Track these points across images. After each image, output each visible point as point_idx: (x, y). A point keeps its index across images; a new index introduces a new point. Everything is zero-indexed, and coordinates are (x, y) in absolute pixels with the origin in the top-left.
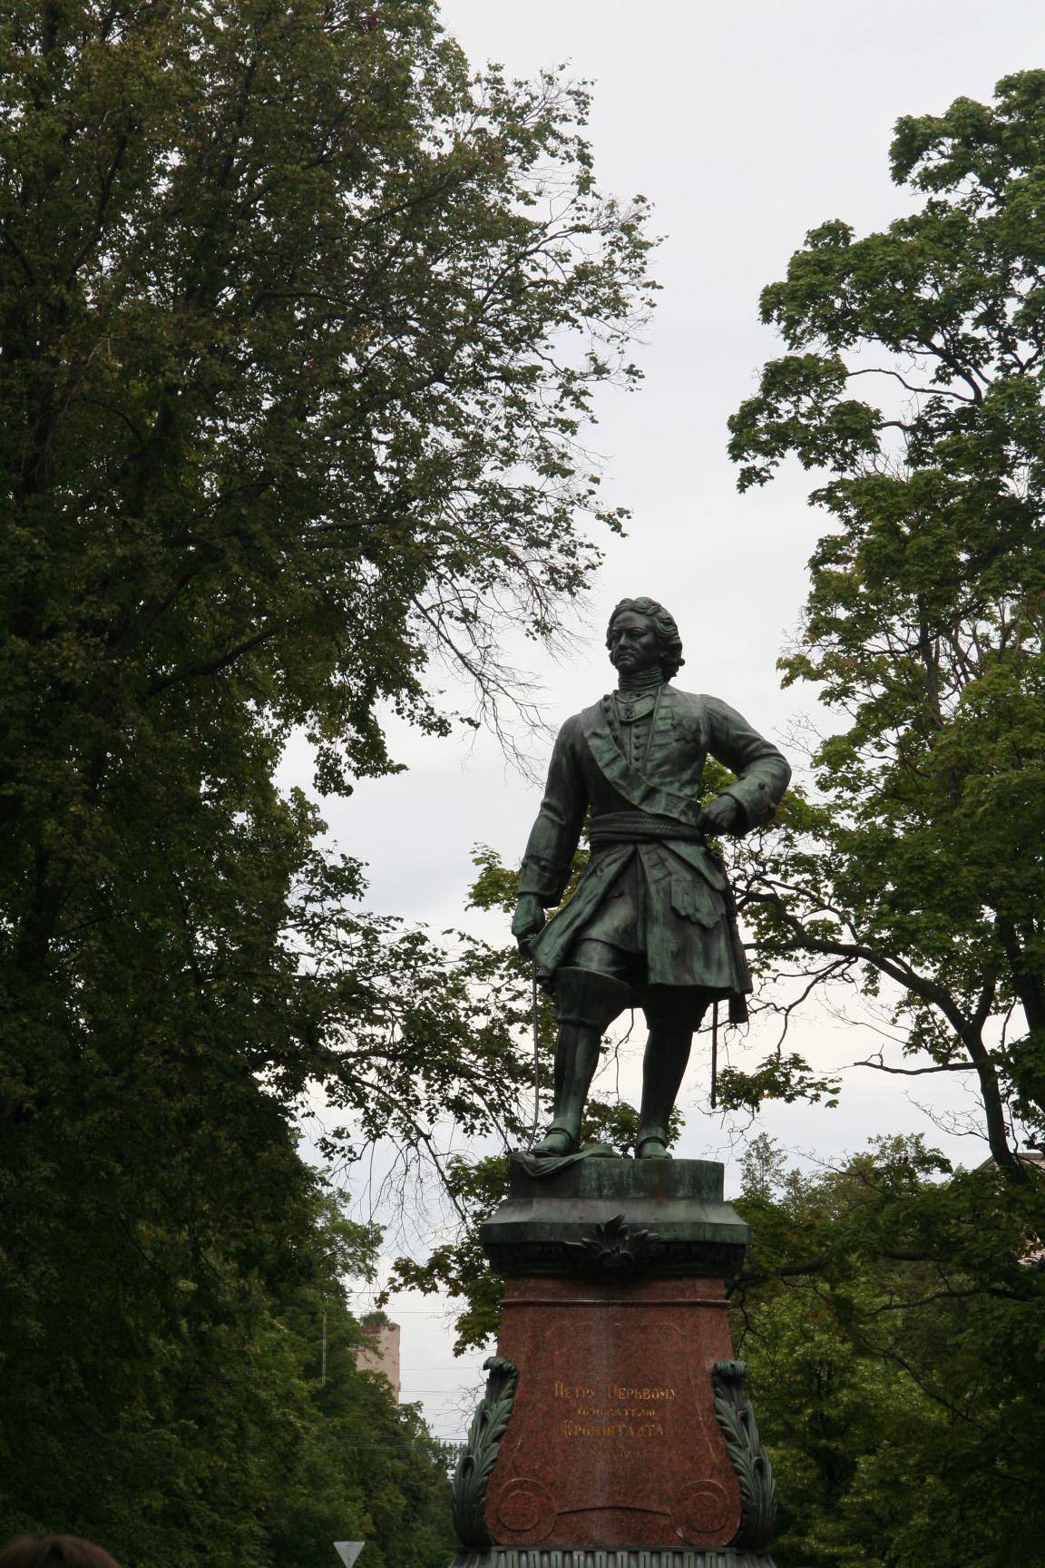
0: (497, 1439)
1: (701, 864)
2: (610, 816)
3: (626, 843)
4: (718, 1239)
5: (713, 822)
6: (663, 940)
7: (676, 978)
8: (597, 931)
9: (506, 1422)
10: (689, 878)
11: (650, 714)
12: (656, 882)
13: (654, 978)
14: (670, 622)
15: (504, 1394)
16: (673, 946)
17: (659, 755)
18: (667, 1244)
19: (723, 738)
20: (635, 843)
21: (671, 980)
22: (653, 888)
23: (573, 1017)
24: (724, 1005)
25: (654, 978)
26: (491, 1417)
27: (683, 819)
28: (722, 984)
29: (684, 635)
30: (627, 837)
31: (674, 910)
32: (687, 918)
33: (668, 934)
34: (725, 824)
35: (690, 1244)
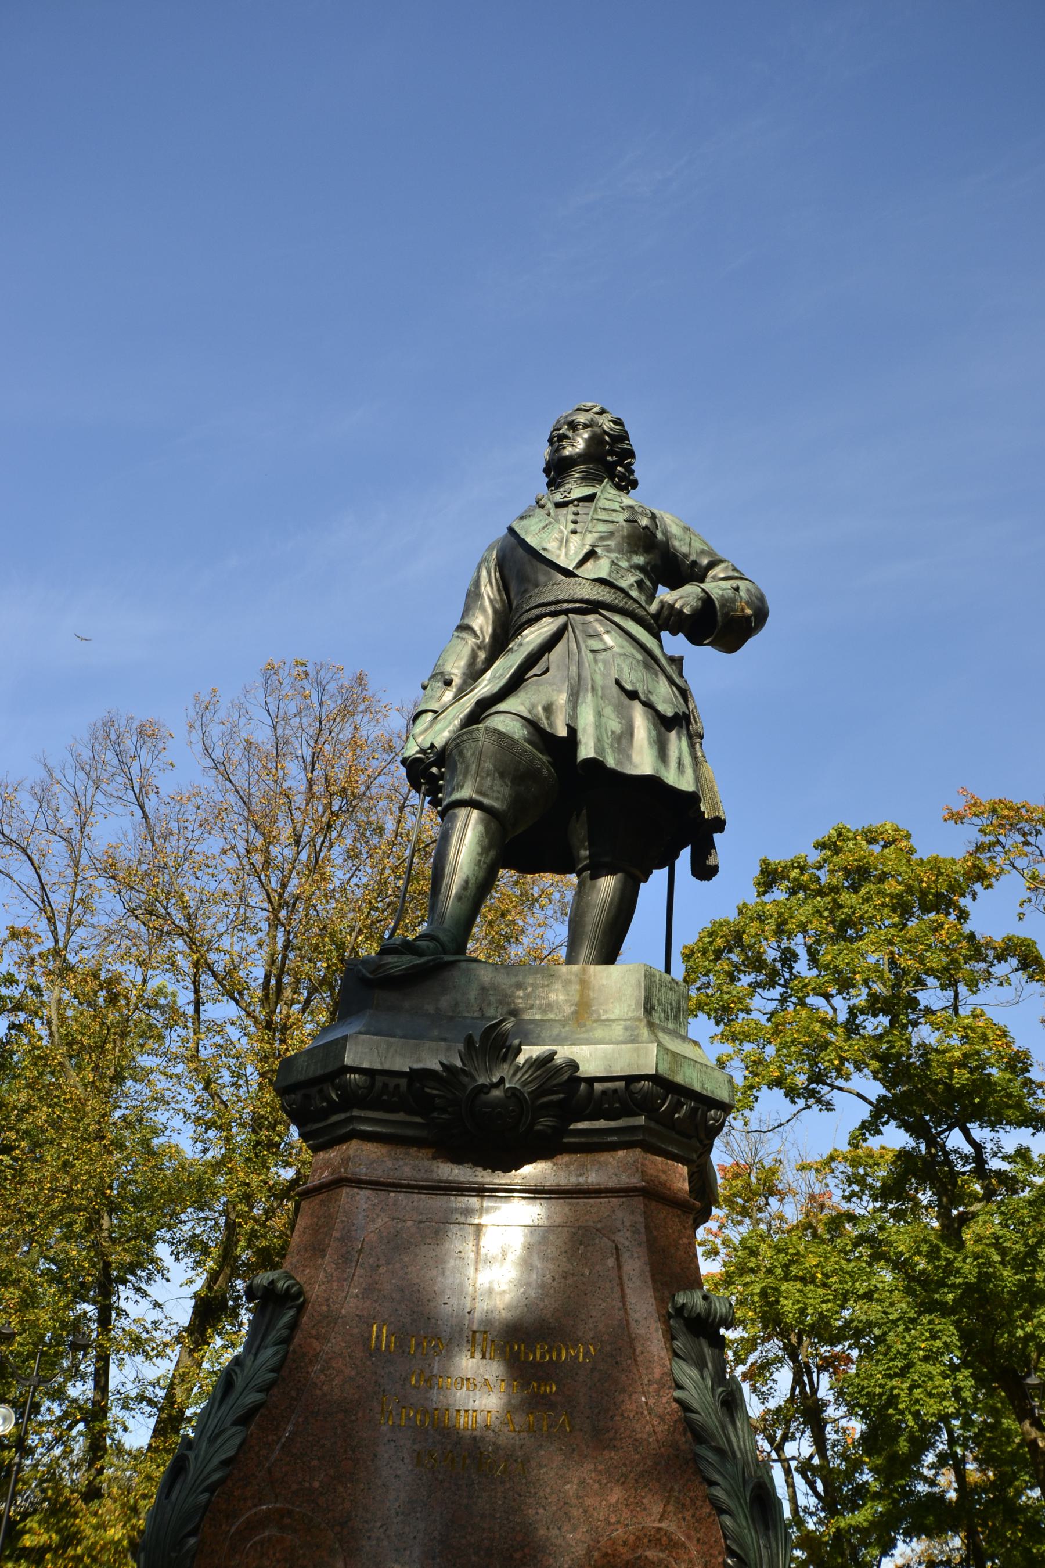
0: (244, 1420)
1: (657, 652)
2: (536, 590)
3: (554, 614)
4: (679, 1079)
5: (672, 607)
6: (599, 715)
7: (619, 762)
8: (509, 704)
9: (267, 1388)
10: (639, 657)
11: (590, 498)
12: (592, 651)
13: (586, 750)
14: (618, 422)
15: (272, 1336)
16: (614, 725)
17: (602, 527)
18: (591, 1081)
19: (684, 549)
20: (566, 612)
21: (611, 762)
22: (588, 657)
23: (466, 792)
24: (685, 856)
25: (586, 750)
26: (239, 1382)
27: (634, 594)
28: (685, 783)
29: (636, 442)
30: (553, 608)
31: (618, 682)
32: (633, 695)
33: (608, 711)
34: (687, 611)
35: (630, 1080)
